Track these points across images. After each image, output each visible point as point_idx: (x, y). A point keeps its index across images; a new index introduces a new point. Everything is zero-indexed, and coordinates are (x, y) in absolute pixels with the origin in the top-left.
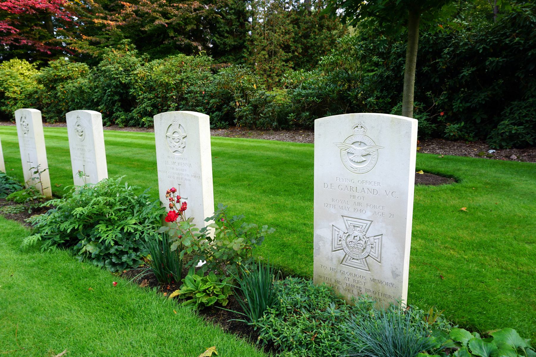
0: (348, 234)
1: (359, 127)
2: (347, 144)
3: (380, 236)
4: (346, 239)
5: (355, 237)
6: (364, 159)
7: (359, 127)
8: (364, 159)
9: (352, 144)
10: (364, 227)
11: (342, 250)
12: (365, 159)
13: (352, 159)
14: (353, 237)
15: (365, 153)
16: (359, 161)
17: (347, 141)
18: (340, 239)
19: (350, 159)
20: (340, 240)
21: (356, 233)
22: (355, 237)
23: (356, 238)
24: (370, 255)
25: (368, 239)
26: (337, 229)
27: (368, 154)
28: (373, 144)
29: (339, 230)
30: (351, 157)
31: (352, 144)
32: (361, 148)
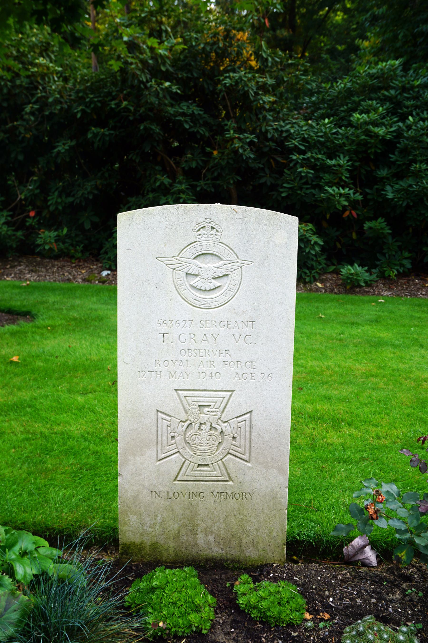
0: (188, 422)
4: (185, 432)
5: (201, 424)
10: (217, 405)
18: (172, 434)
20: (173, 437)
21: (204, 417)
23: (203, 427)
25: (226, 424)
26: (164, 416)
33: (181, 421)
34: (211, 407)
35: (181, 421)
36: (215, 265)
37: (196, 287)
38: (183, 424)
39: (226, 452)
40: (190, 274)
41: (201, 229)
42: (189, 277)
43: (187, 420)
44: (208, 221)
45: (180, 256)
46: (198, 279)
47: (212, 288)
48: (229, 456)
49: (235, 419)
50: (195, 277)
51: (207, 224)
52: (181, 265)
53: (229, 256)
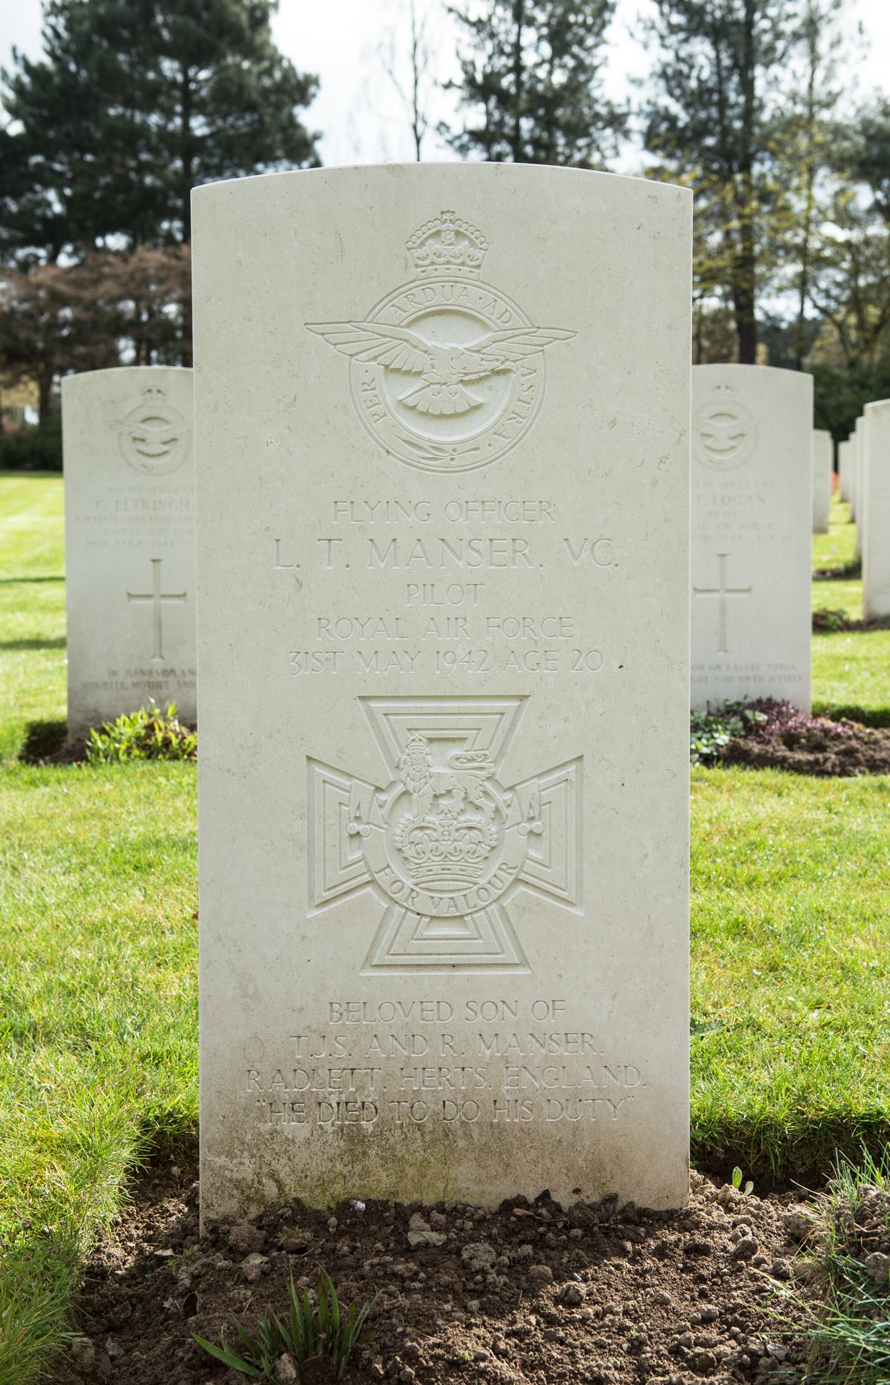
0: (400, 788)
2: (384, 329)
3: (572, 768)
5: (436, 797)
11: (369, 889)
13: (410, 403)
14: (428, 800)
16: (448, 411)
22: (436, 797)
23: (443, 802)
24: (523, 876)
25: (508, 796)
29: (346, 782)
31: (409, 325)
33: (378, 789)
34: (467, 745)
35: (378, 789)
36: (467, 346)
38: (382, 797)
39: (511, 878)
40: (397, 371)
41: (430, 241)
43: (393, 783)
46: (419, 383)
47: (460, 410)
48: (521, 888)
49: (535, 780)
51: (444, 227)
53: (504, 318)
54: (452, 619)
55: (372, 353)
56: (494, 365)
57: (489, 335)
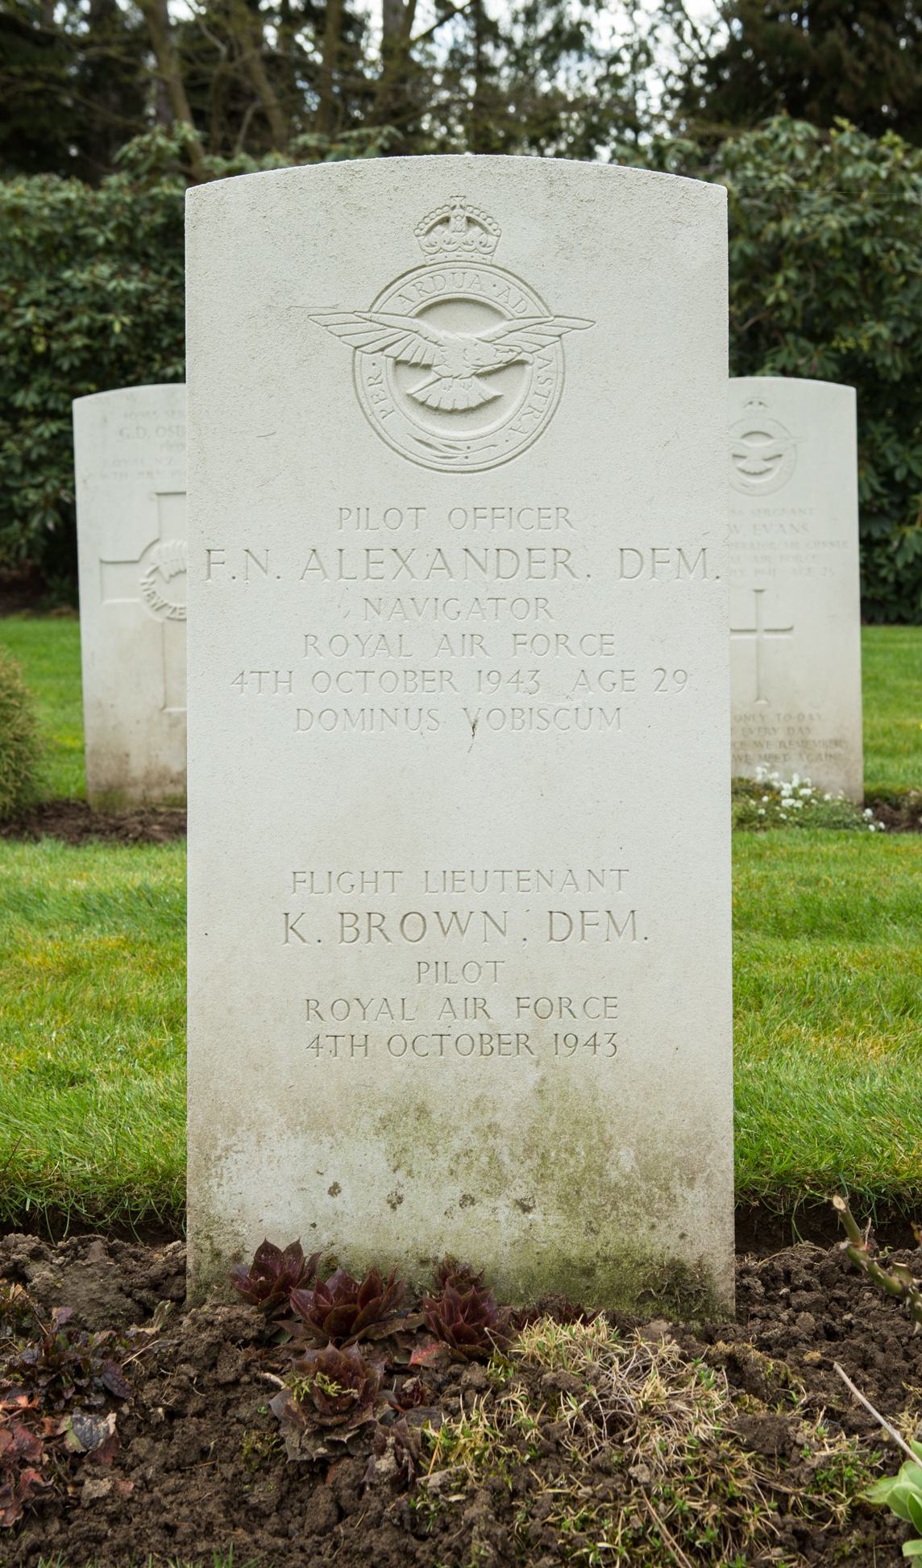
1: (458, 223)
6: (489, 389)
7: (458, 223)
8: (489, 389)
9: (420, 314)
12: (493, 392)
13: (422, 400)
15: (492, 358)
16: (461, 406)
17: (393, 304)
19: (409, 395)
27: (510, 364)
28: (533, 308)
30: (417, 383)
31: (420, 314)
32: (468, 336)
36: (481, 335)
37: (423, 404)
40: (405, 363)
42: (404, 371)
44: (457, 202)
45: (374, 310)
50: (422, 373)
52: (381, 334)
54: (468, 637)
55: (381, 344)
56: (509, 357)
57: (504, 324)
